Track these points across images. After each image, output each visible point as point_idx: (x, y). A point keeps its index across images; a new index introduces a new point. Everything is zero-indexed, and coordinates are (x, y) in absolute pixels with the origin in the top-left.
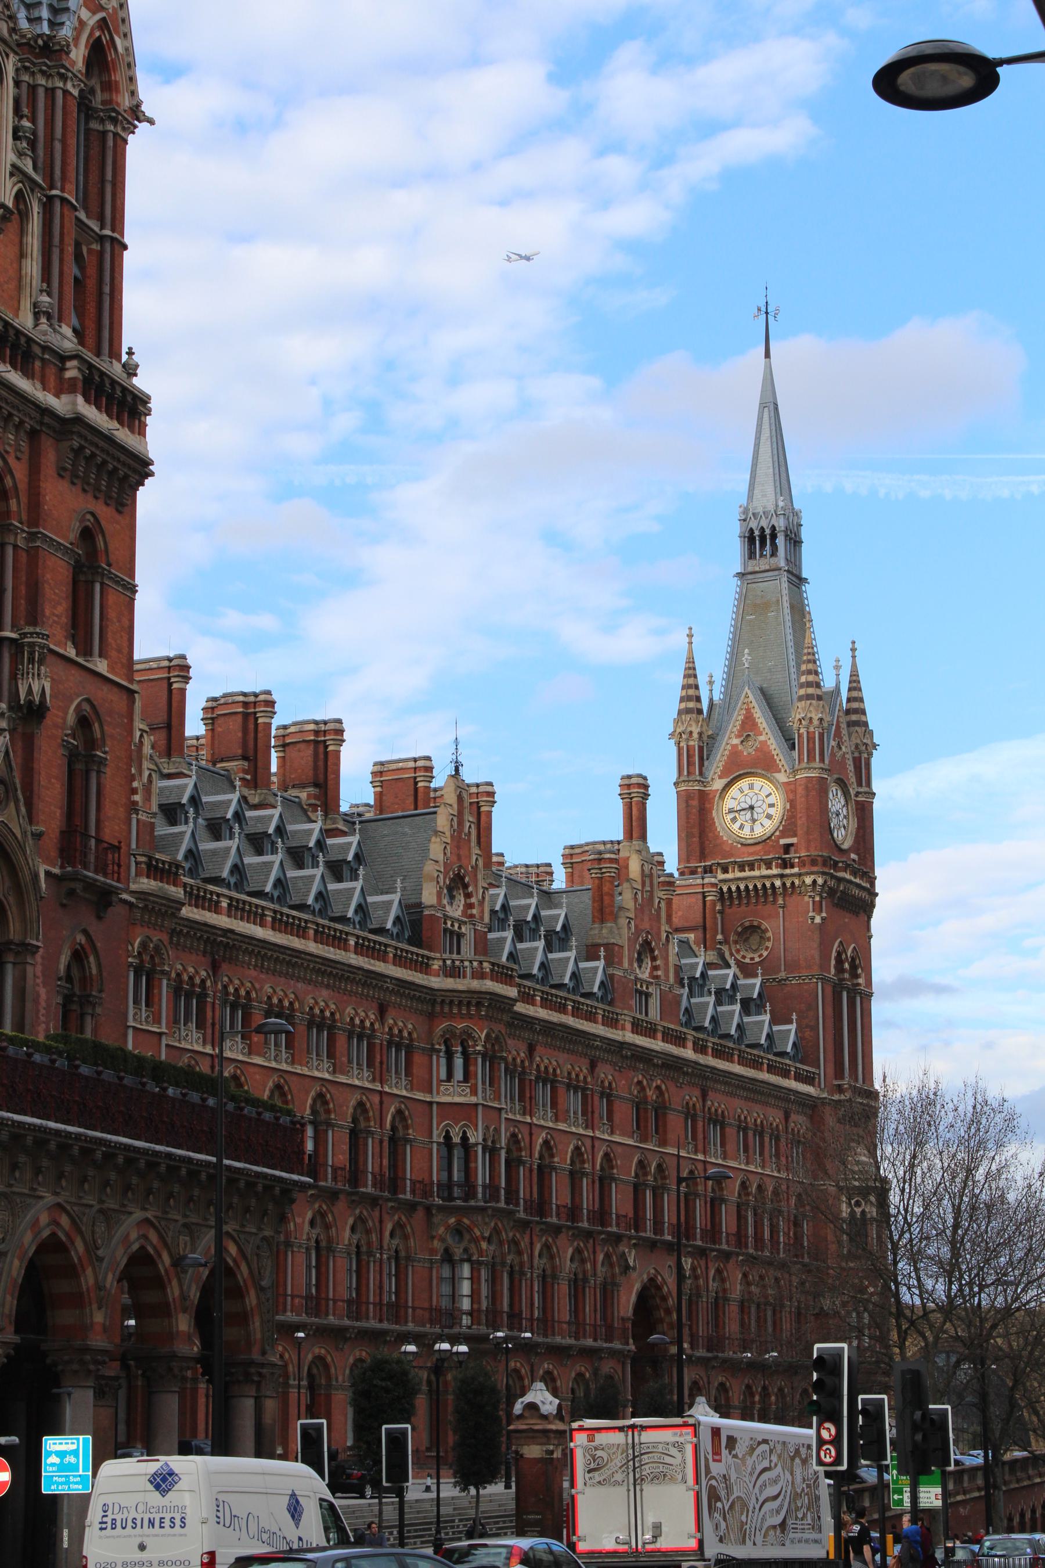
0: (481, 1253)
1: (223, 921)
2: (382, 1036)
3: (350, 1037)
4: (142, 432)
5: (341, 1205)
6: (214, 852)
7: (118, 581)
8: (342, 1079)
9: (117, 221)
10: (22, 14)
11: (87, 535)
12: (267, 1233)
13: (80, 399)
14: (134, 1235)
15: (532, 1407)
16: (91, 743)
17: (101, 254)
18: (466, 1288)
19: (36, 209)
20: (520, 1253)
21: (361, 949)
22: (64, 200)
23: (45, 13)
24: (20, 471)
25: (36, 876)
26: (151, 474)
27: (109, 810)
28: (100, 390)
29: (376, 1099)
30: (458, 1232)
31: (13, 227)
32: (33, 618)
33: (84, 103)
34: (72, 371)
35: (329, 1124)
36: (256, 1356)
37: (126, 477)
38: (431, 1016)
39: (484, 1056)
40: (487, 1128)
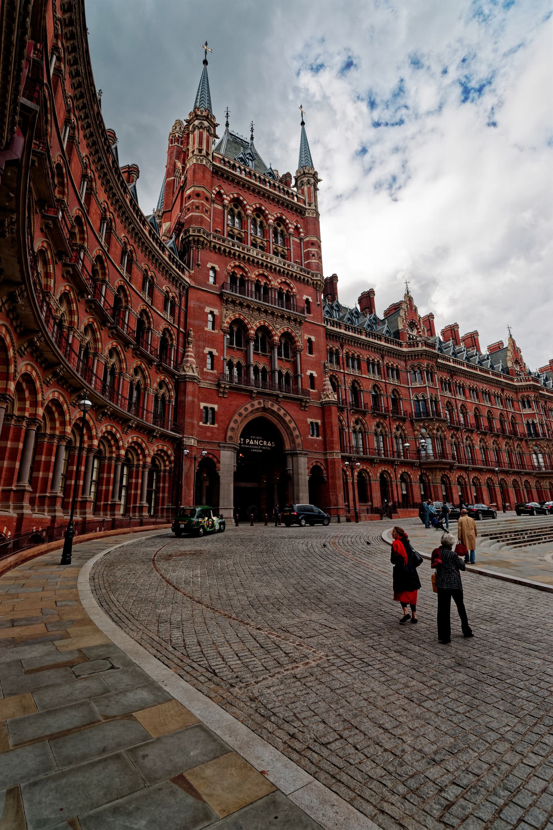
1: (452, 364)
5: (500, 439)
18: (541, 460)
35: (493, 418)
38: (517, 393)
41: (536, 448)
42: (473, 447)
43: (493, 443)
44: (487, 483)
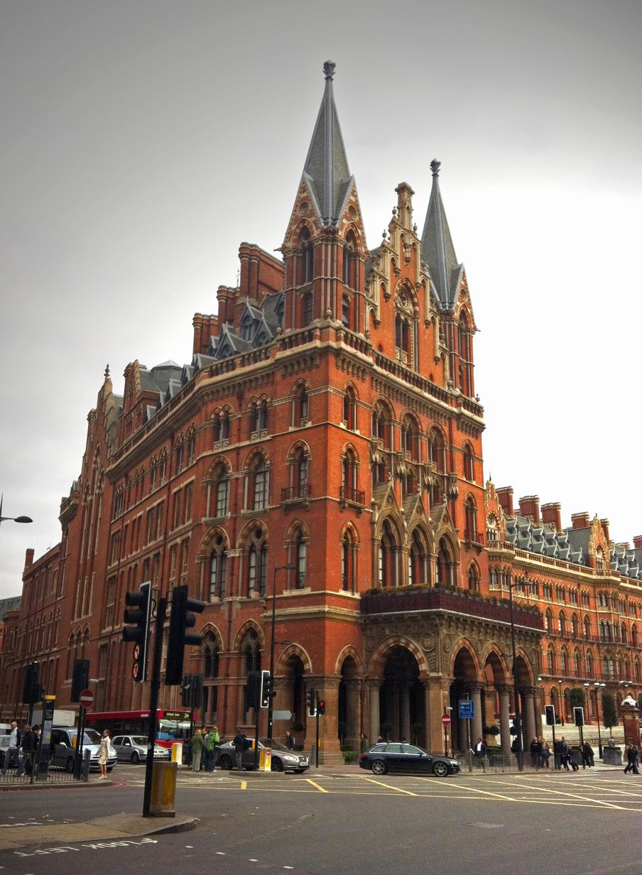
0: (615, 657)
1: (528, 560)
2: (579, 594)
3: (570, 594)
4: (482, 416)
5: (570, 643)
6: (524, 541)
7: (477, 459)
8: (568, 606)
9: (471, 359)
10: (441, 305)
11: (467, 446)
12: (534, 647)
13: (462, 408)
14: (490, 648)
15: (627, 703)
16: (472, 505)
17: (467, 368)
18: (612, 668)
19: (447, 357)
20: (628, 658)
21: (570, 568)
22: (455, 354)
23: (447, 304)
24: (446, 429)
25: (458, 543)
26: (484, 428)
27: (479, 524)
28: (468, 405)
29: (579, 612)
30: (608, 651)
31: (440, 363)
32: (452, 469)
33: (460, 328)
34: (460, 401)
36: (532, 685)
37: (478, 429)
38: (594, 587)
39: (612, 598)
40: (614, 620)
41: (606, 654)
42: (541, 653)
43: (562, 648)
44: (552, 692)
